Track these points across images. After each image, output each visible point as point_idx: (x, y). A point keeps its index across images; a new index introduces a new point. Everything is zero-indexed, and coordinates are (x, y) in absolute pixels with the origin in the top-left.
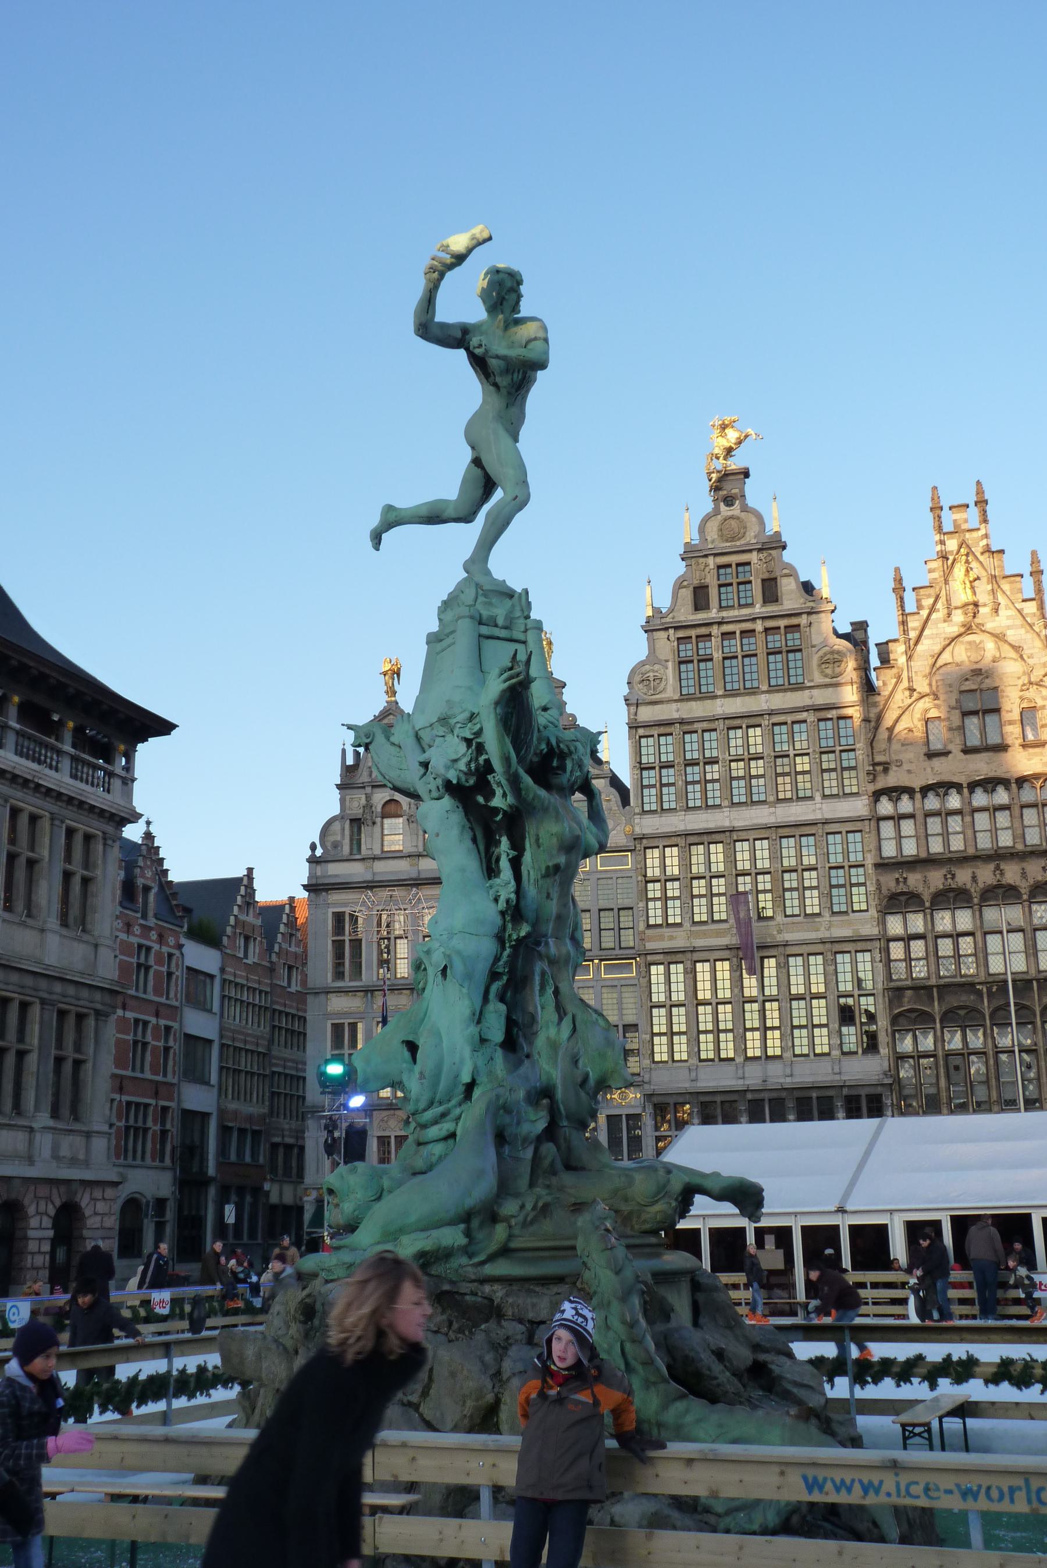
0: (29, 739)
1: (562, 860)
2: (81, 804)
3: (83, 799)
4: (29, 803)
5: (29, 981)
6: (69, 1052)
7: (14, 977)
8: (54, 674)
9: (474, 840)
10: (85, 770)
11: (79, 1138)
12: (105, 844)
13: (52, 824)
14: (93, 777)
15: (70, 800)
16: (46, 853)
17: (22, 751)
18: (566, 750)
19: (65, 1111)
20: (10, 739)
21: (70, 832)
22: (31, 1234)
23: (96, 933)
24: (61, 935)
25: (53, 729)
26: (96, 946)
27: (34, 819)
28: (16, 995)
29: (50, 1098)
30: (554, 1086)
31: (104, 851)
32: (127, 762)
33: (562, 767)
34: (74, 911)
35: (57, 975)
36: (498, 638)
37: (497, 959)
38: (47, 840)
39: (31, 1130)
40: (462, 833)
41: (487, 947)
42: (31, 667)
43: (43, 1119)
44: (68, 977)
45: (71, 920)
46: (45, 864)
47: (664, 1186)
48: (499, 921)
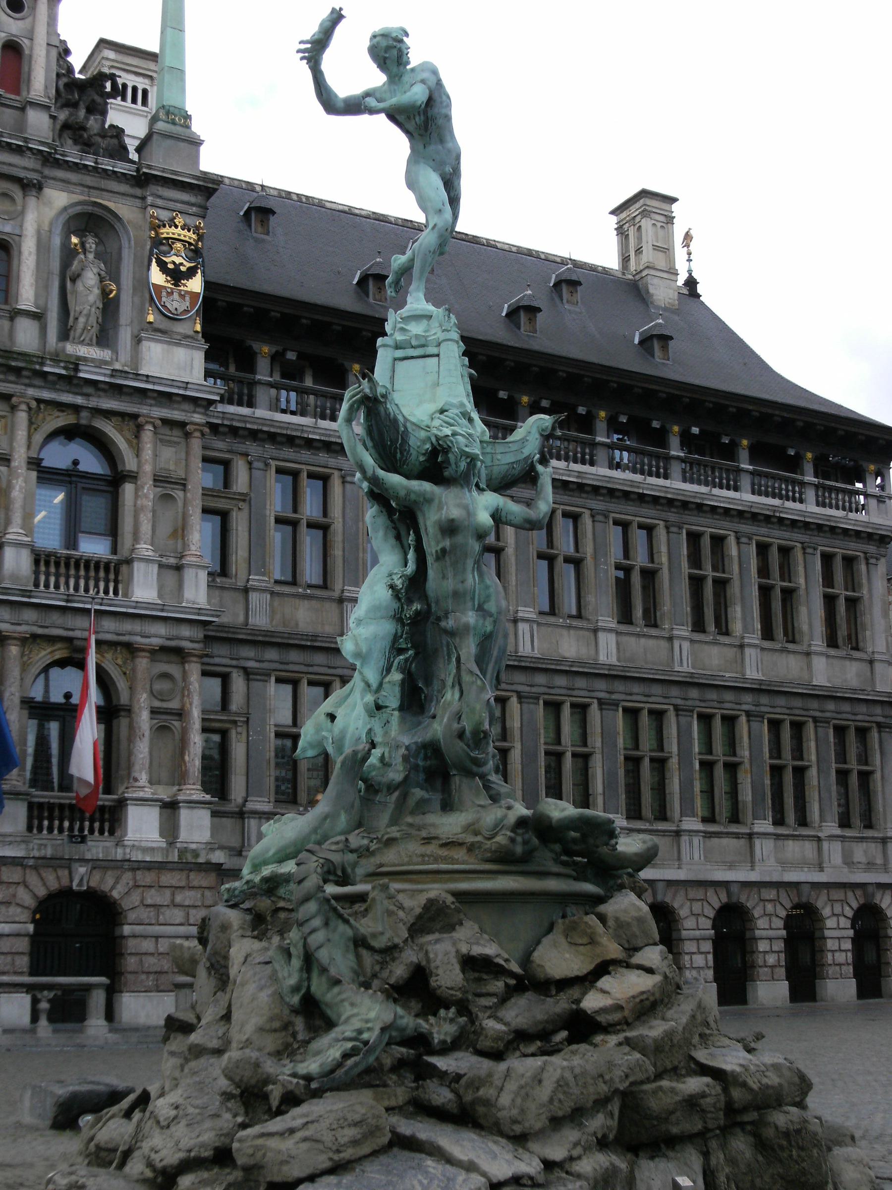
0: (773, 478)
1: (447, 543)
2: (833, 529)
3: (833, 524)
4: (776, 537)
5: (797, 703)
6: (853, 765)
7: (781, 701)
8: (777, 412)
9: (398, 538)
10: (840, 497)
11: (873, 845)
12: (867, 564)
13: (804, 553)
14: (850, 503)
15: (820, 527)
16: (802, 581)
17: (760, 490)
18: (445, 446)
19: (856, 820)
20: (745, 481)
21: (827, 559)
22: (827, 933)
23: (870, 650)
24: (828, 656)
25: (794, 465)
26: (871, 662)
27: (785, 551)
28: (786, 717)
29: (835, 809)
30: (439, 740)
31: (868, 568)
32: (882, 480)
33: (447, 461)
34: (842, 631)
35: (826, 693)
36: (412, 357)
37: (396, 638)
38: (801, 569)
39: (819, 839)
40: (386, 534)
41: (387, 628)
42: (751, 411)
43: (831, 828)
44: (838, 695)
45: (840, 641)
46: (802, 592)
47: (502, 820)
48: (395, 605)
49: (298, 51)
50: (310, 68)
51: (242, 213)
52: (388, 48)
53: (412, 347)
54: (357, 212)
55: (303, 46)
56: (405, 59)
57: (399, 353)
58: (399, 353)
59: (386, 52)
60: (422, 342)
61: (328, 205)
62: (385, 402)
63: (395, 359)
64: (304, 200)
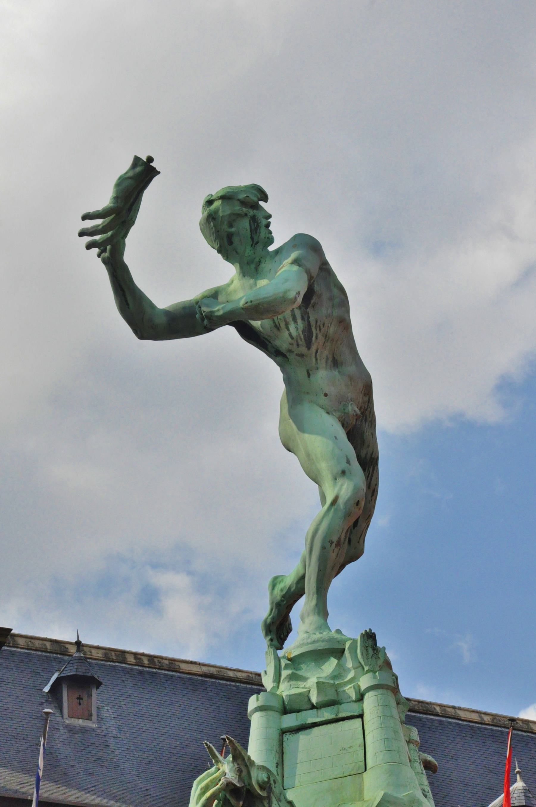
49: (82, 234)
50: (104, 262)
51: (47, 689)
52: (234, 218)
53: (313, 707)
54: (231, 674)
55: (90, 224)
56: (263, 233)
57: (290, 721)
58: (290, 721)
59: (231, 225)
60: (331, 696)
61: (184, 667)
62: (269, 798)
63: (283, 732)
64: (146, 662)
